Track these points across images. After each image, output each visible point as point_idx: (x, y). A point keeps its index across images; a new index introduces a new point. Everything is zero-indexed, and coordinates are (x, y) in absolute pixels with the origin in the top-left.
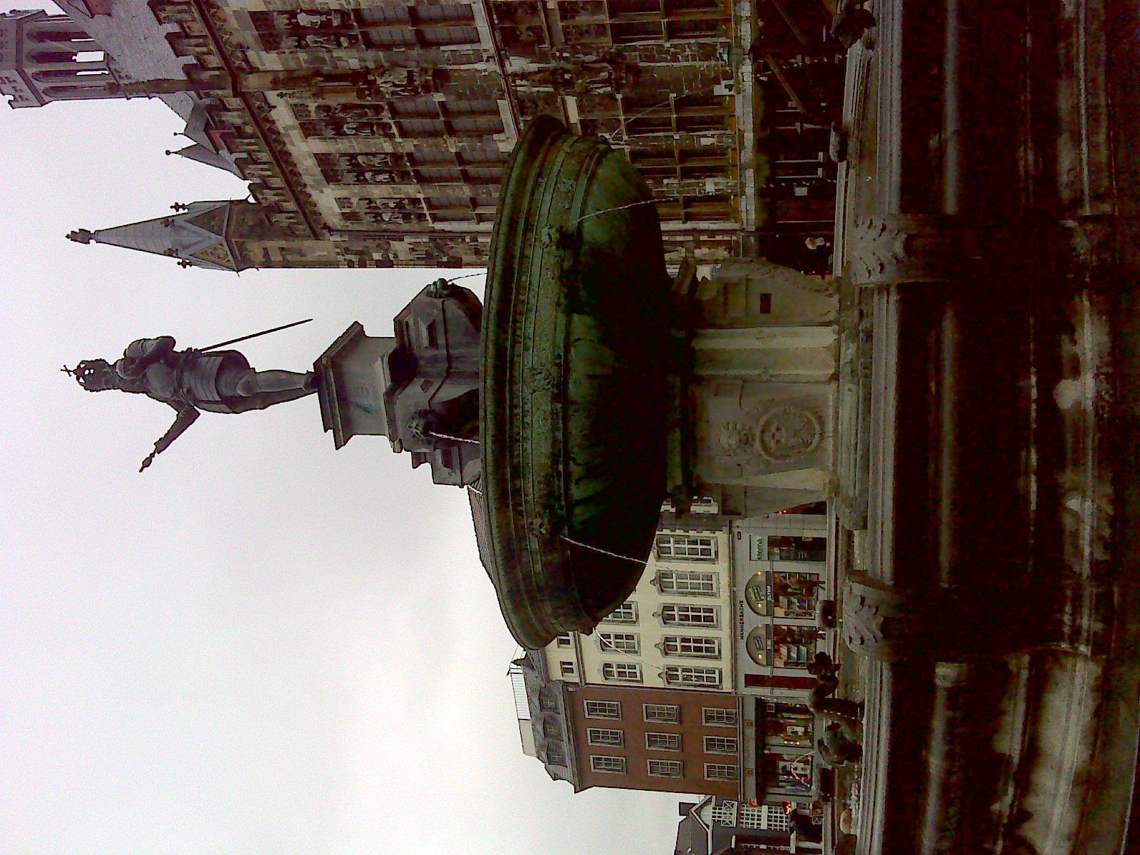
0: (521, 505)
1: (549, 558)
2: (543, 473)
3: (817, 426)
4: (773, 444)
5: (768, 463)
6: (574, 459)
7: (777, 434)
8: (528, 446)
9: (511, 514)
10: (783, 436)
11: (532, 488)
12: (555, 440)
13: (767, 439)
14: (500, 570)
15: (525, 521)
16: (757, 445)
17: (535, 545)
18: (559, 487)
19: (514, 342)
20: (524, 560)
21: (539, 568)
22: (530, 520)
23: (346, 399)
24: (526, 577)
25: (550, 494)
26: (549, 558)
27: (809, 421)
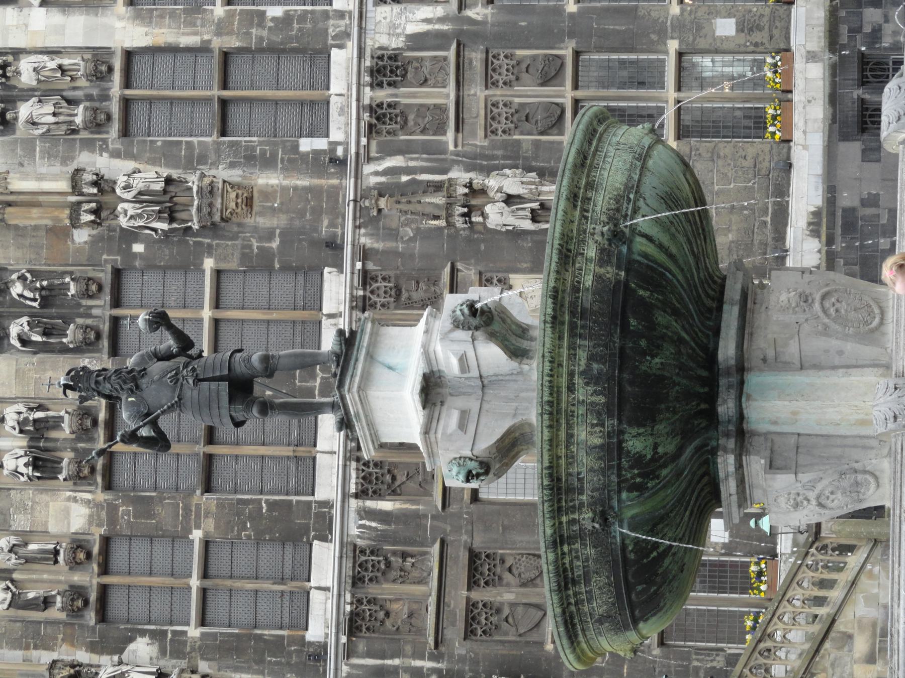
0: (587, 211)
1: (602, 271)
2: (615, 193)
3: (877, 311)
4: (832, 311)
5: (826, 327)
6: (644, 199)
7: (838, 305)
8: (606, 174)
9: (577, 213)
10: (843, 307)
11: (601, 202)
12: (630, 178)
13: (827, 304)
14: (554, 254)
15: (589, 227)
16: (817, 306)
17: (591, 252)
18: (627, 208)
19: (605, 131)
20: (577, 265)
21: (588, 281)
22: (593, 226)
23: (372, 357)
24: (576, 289)
25: (618, 210)
26: (602, 271)
27: (869, 306)
